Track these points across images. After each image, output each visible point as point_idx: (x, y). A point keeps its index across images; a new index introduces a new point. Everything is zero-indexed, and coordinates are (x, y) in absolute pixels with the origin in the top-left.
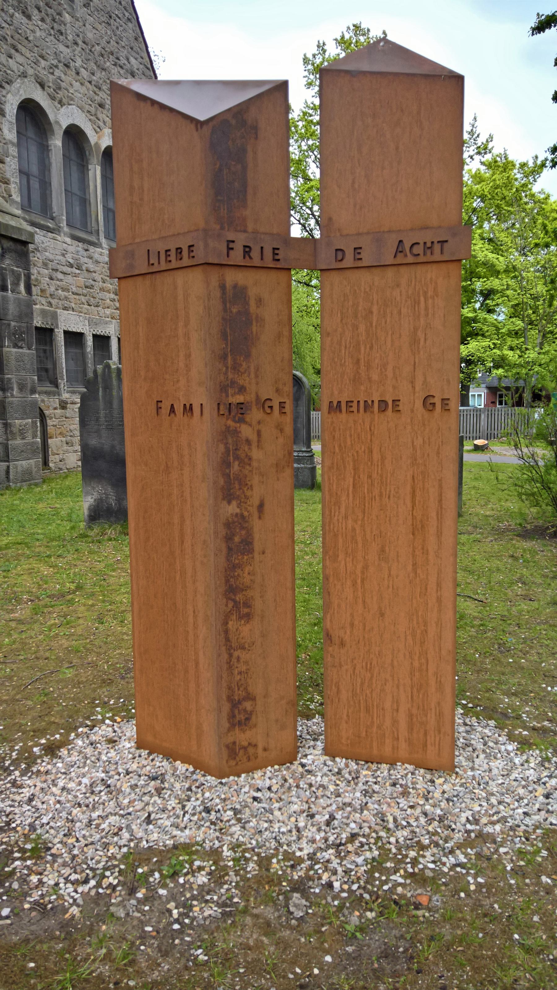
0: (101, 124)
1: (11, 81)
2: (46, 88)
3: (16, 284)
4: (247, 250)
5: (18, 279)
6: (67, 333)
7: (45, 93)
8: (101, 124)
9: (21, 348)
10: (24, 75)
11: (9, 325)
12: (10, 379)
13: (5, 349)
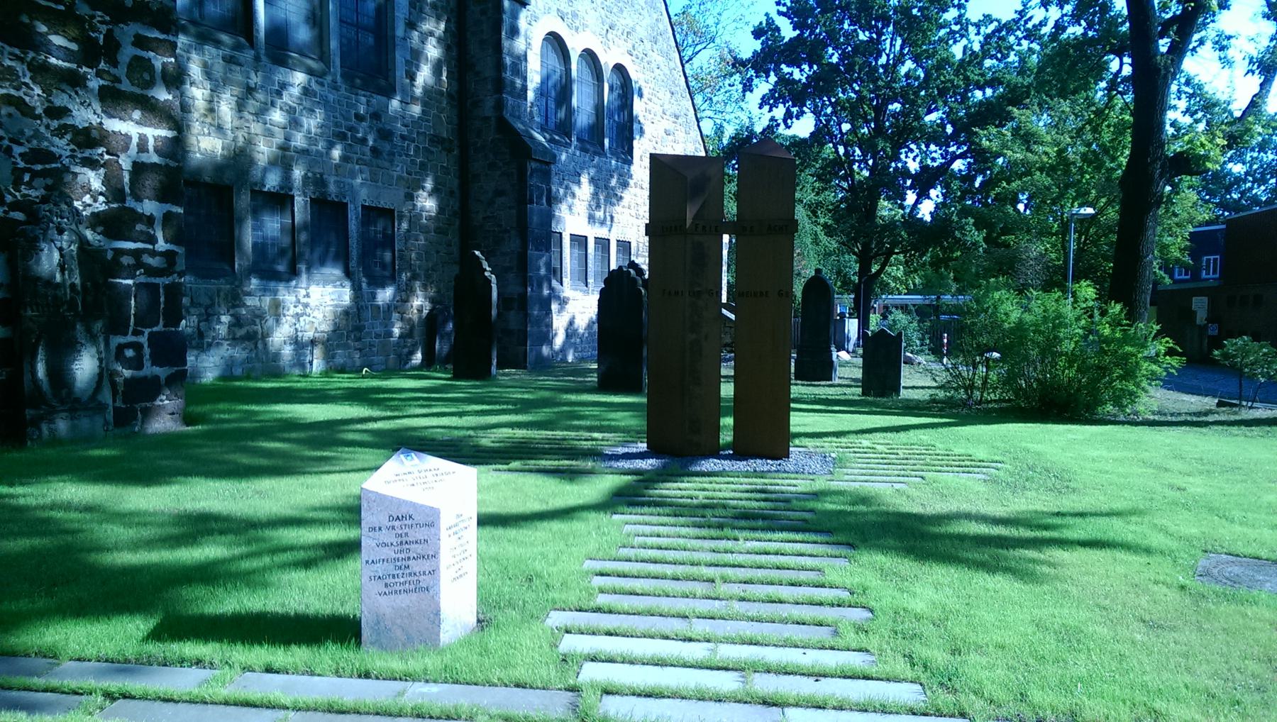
0: (611, 43)
1: (538, 18)
2: (565, 19)
3: (540, 197)
4: (704, 227)
5: (542, 195)
6: (574, 238)
7: (565, 24)
8: (611, 43)
9: (542, 251)
10: (548, 11)
11: (533, 231)
12: (531, 277)
13: (529, 252)
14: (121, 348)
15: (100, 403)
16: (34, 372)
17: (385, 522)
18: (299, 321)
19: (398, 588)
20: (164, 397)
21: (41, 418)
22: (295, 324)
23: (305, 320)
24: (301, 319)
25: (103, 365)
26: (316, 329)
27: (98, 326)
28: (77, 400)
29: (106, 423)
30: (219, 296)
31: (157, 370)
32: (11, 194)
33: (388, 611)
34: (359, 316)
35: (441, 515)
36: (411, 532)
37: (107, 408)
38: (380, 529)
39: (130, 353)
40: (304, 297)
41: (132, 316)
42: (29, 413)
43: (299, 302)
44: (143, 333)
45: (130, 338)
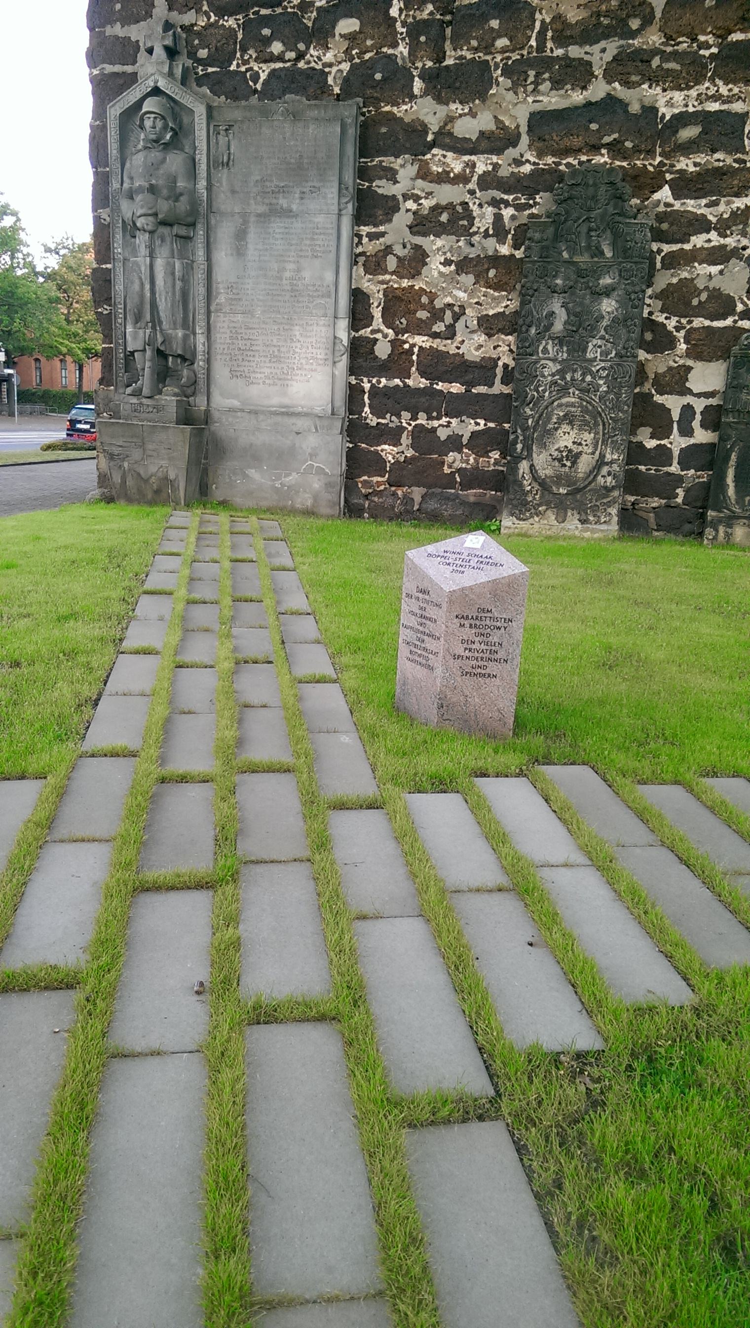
21: (720, 521)
32: (743, 303)
42: (711, 514)
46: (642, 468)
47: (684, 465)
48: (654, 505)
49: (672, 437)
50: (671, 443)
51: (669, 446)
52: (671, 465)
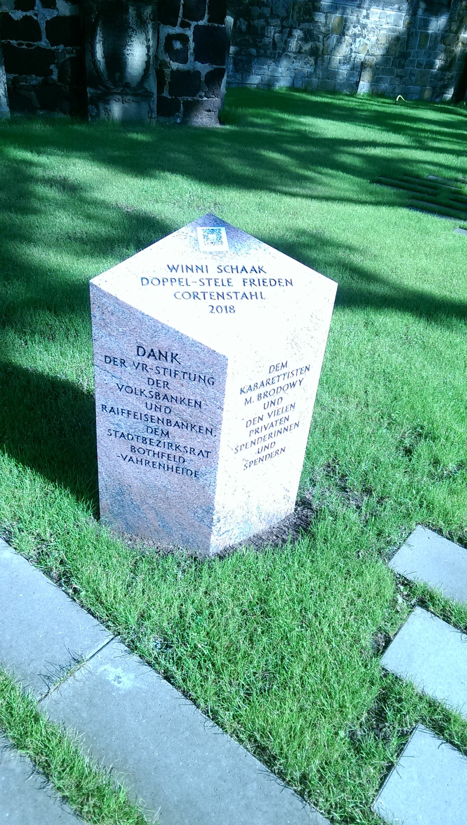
14: (170, 38)
15: (147, 91)
16: (93, 54)
17: (131, 355)
18: (355, 42)
19: (150, 458)
20: (204, 94)
22: (351, 45)
23: (360, 41)
24: (357, 40)
25: (151, 54)
26: (368, 51)
27: (148, 11)
28: (127, 85)
29: (151, 111)
30: (293, 9)
31: (199, 66)
33: (136, 483)
34: (407, 42)
35: (229, 371)
36: (174, 382)
37: (152, 97)
38: (123, 362)
39: (178, 45)
40: (364, 18)
41: (181, 7)
42: (90, 91)
43: (359, 23)
44: (189, 26)
45: (177, 30)
46: (13, 42)
47: (53, 41)
48: (34, 82)
49: (36, 8)
50: (36, 15)
51: (35, 18)
52: (40, 39)
